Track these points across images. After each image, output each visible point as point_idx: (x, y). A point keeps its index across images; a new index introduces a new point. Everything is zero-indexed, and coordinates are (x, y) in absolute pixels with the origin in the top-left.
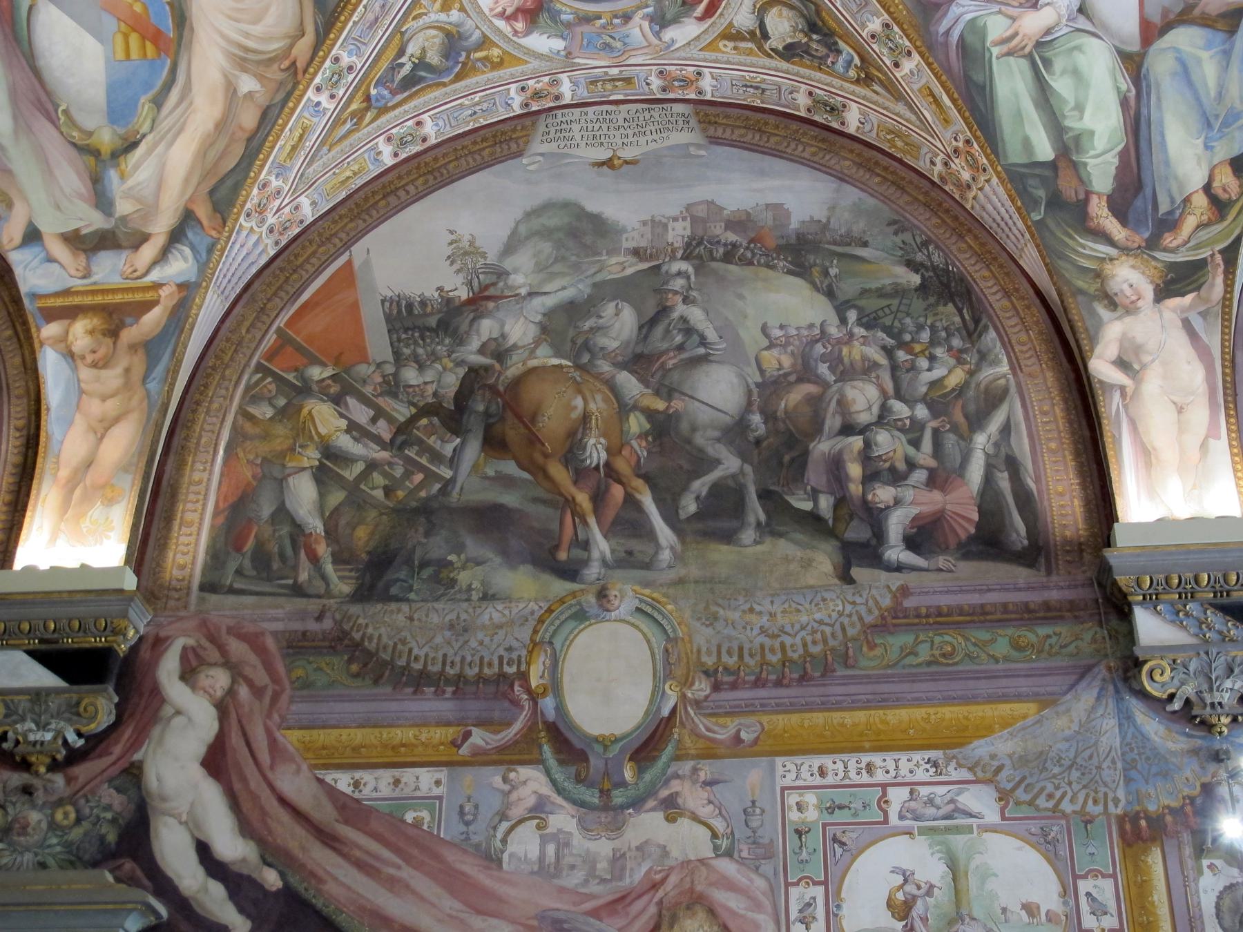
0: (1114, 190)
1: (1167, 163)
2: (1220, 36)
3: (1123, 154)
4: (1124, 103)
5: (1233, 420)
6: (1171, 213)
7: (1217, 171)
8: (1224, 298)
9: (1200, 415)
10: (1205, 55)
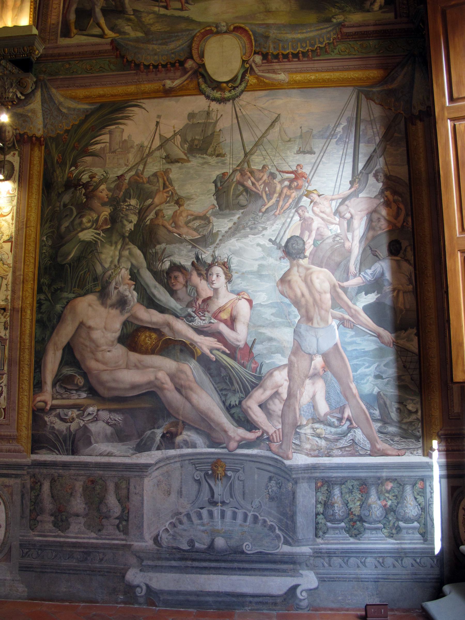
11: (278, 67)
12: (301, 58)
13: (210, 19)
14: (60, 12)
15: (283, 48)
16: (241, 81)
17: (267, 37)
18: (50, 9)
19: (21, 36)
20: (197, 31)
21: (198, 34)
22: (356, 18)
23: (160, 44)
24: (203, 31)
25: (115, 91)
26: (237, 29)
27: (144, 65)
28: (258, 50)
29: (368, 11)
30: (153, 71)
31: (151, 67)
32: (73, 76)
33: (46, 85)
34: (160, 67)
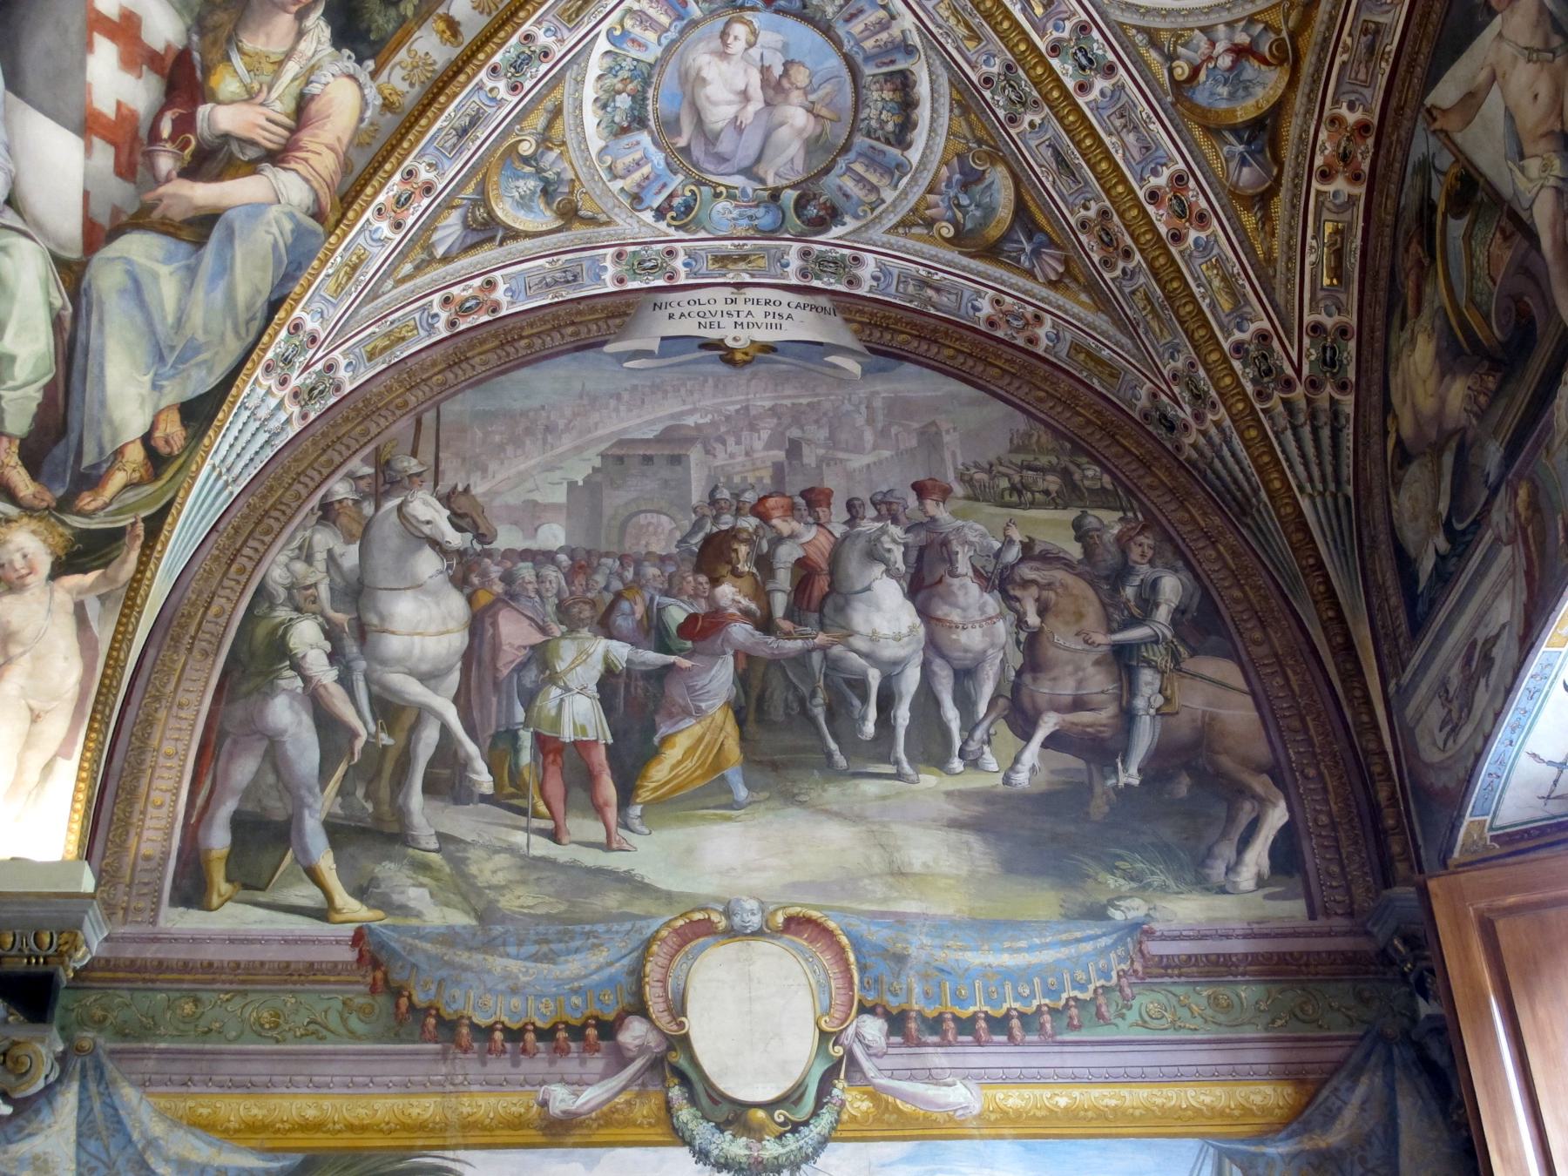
0: (30, 433)
1: (103, 404)
2: (184, 248)
3: (49, 390)
4: (57, 322)
5: (93, 735)
6: (96, 466)
7: (163, 417)
8: (133, 579)
9: (57, 726)
10: (164, 270)
11: (942, 1061)
12: (1017, 1032)
13: (704, 884)
14: (174, 819)
15: (958, 999)
16: (819, 1105)
17: (901, 959)
18: (139, 807)
19: (39, 895)
20: (661, 921)
21: (664, 933)
22: (1185, 910)
23: (535, 958)
24: (681, 922)
25: (362, 1112)
26: (796, 924)
27: (474, 1027)
28: (871, 998)
29: (1222, 890)
30: (504, 1051)
31: (498, 1035)
32: (208, 1047)
33: (99, 1068)
34: (530, 1037)
